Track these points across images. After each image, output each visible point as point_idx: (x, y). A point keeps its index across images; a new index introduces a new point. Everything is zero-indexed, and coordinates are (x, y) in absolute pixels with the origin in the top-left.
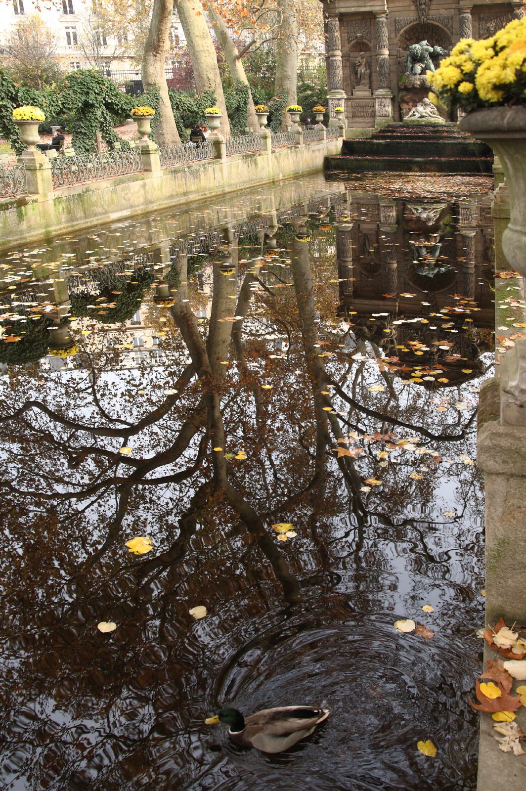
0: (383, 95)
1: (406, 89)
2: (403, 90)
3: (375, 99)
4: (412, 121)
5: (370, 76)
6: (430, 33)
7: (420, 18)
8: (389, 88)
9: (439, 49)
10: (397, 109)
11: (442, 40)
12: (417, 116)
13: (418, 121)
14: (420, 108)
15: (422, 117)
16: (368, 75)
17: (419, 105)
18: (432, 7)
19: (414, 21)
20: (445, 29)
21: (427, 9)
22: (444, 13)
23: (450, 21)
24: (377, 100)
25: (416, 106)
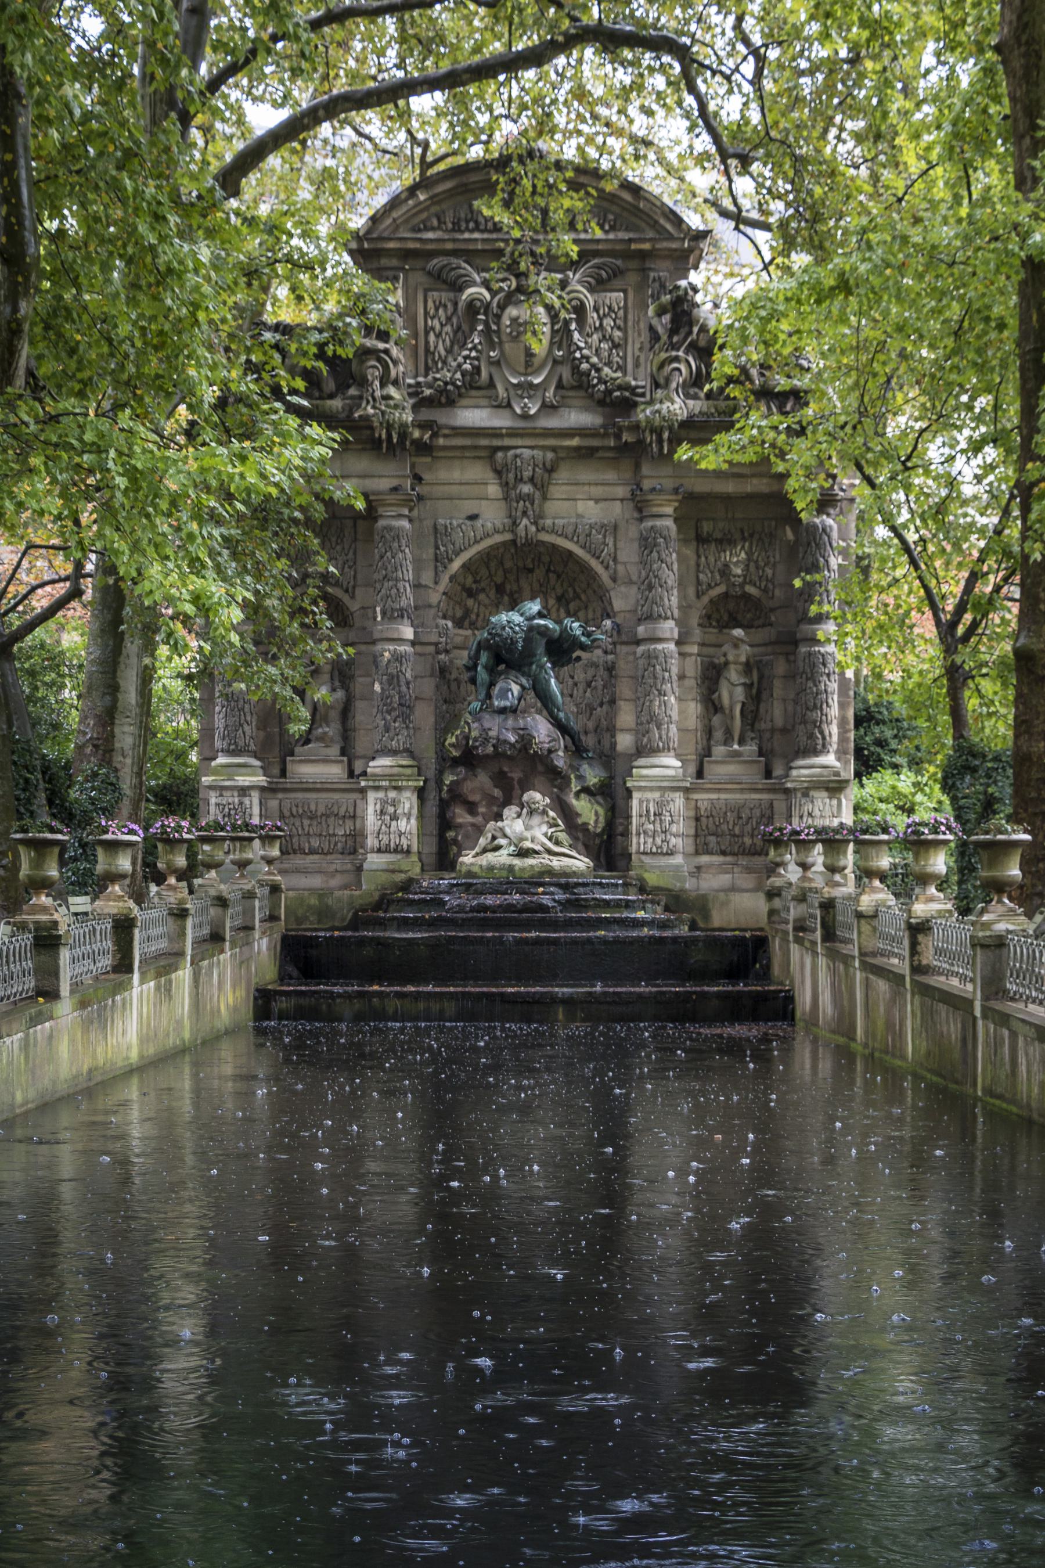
0: (391, 777)
1: (469, 759)
2: (456, 762)
3: (363, 791)
4: (491, 868)
5: (346, 711)
6: (539, 573)
7: (515, 524)
8: (410, 753)
9: (576, 627)
10: (433, 828)
11: (577, 596)
12: (504, 852)
13: (511, 868)
14: (513, 824)
15: (523, 853)
16: (340, 707)
17: (510, 812)
18: (555, 491)
19: (497, 531)
20: (594, 563)
21: (537, 494)
22: (591, 511)
23: (610, 541)
24: (371, 796)
25: (499, 817)
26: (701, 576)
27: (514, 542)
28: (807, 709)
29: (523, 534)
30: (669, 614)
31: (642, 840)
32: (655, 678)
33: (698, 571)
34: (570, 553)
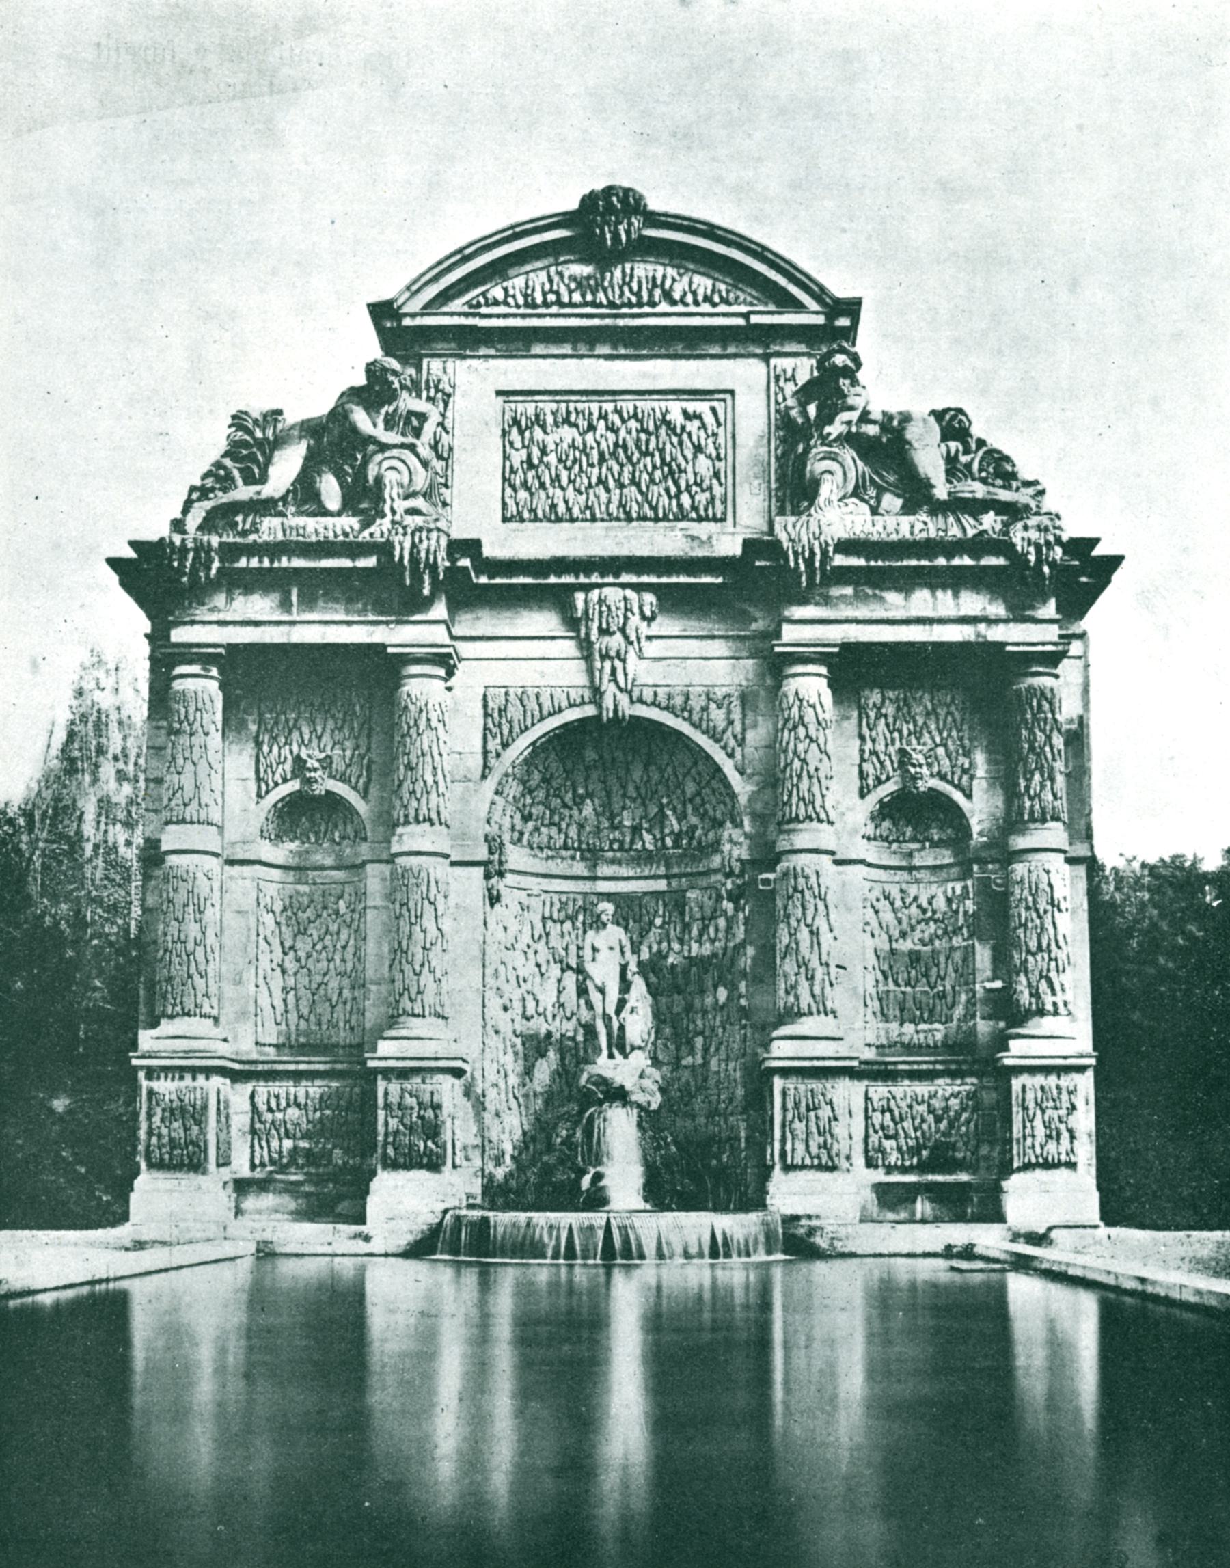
26: (865, 765)
27: (598, 718)
28: (1029, 952)
29: (611, 707)
30: (823, 816)
31: (788, 1147)
32: (804, 908)
33: (863, 760)
34: (679, 734)
